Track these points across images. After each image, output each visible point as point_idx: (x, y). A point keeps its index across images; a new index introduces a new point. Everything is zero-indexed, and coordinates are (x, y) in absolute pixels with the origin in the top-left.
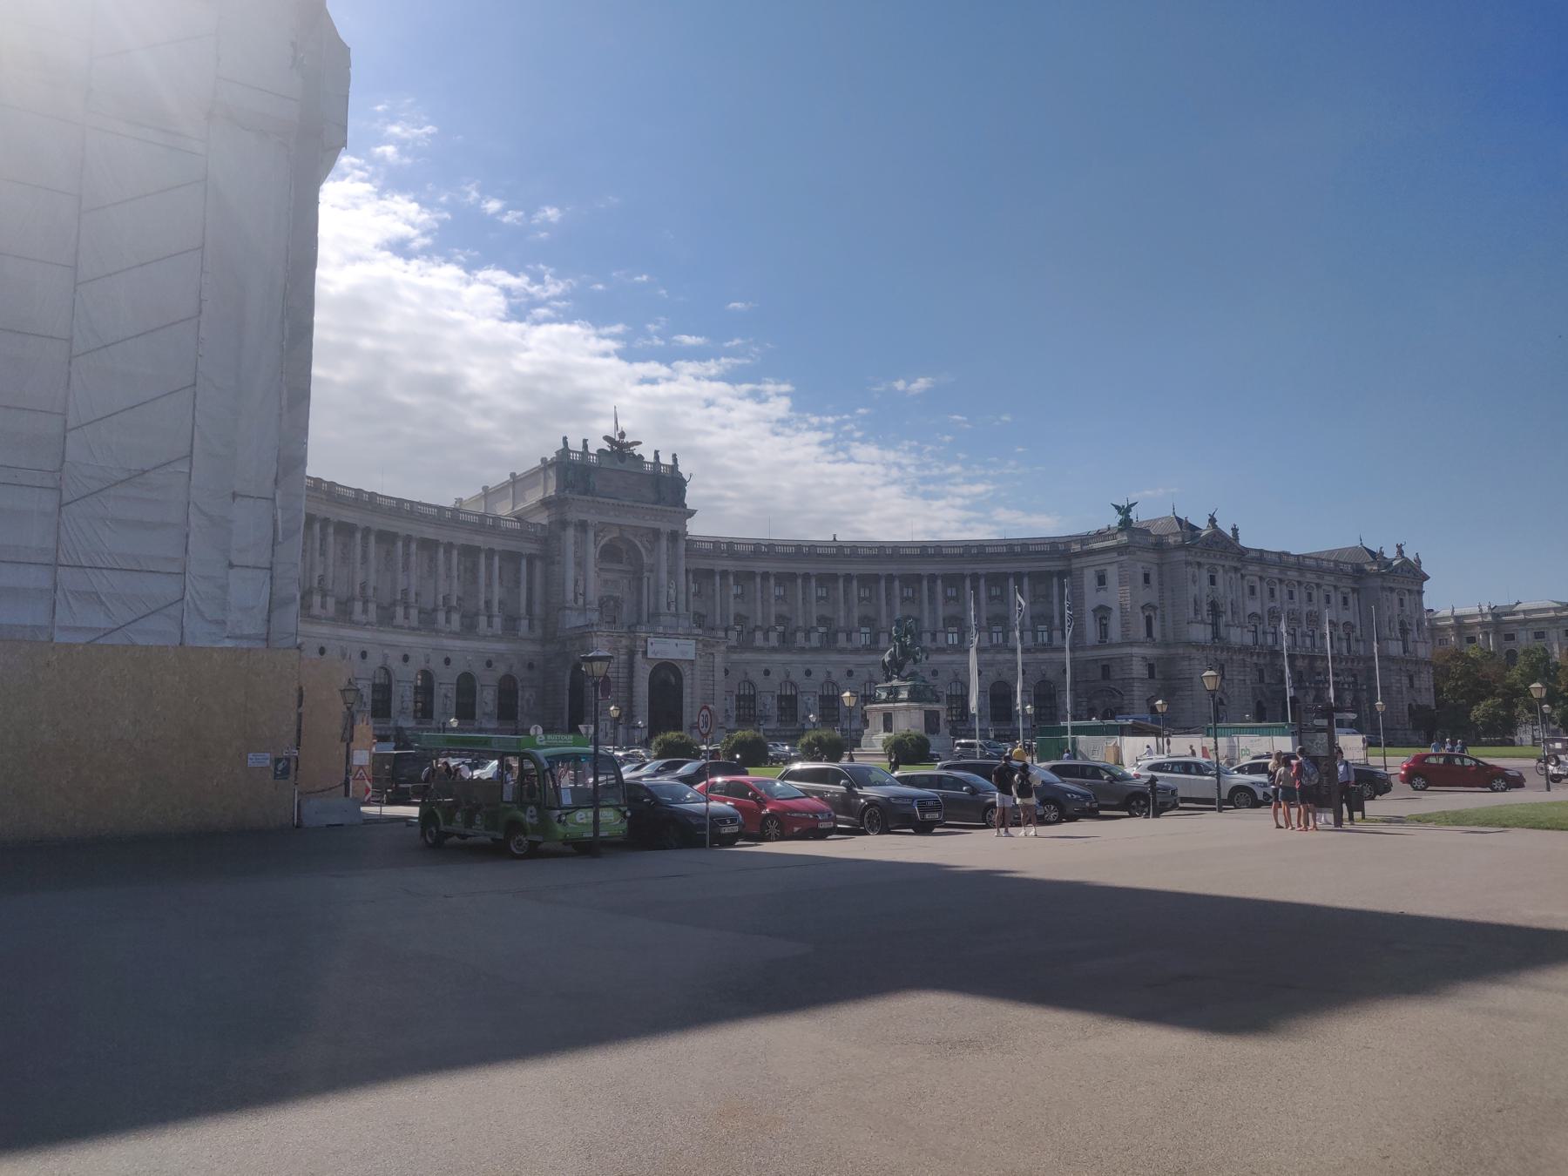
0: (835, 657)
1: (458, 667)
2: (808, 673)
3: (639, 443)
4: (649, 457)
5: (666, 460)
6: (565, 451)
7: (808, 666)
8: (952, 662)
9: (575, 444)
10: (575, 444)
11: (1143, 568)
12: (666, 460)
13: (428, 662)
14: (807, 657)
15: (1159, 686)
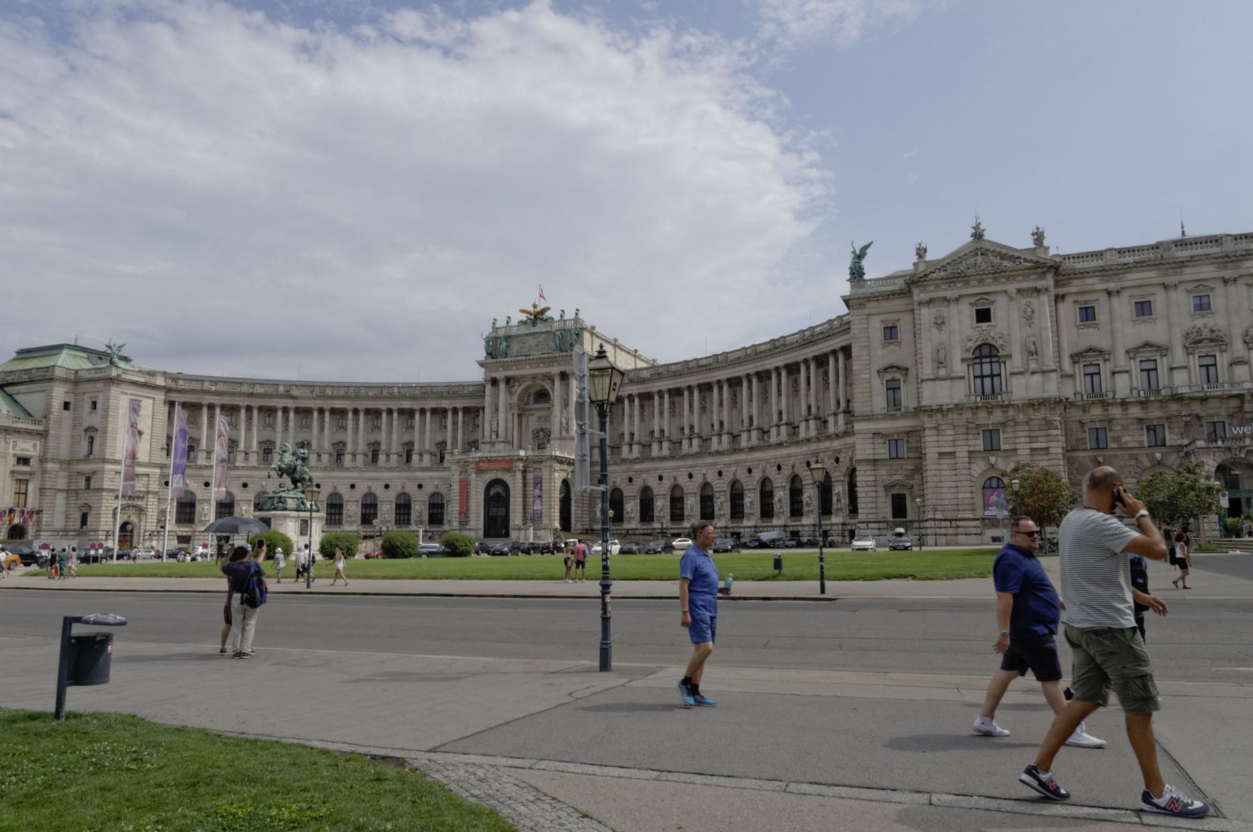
0: (709, 460)
1: (429, 489)
2: (690, 476)
3: (548, 309)
4: (557, 318)
5: (570, 315)
6: (495, 329)
7: (690, 470)
8: (790, 456)
9: (501, 323)
10: (501, 323)
11: (882, 322)
12: (570, 315)
13: (403, 487)
14: (690, 462)
15: (912, 467)
